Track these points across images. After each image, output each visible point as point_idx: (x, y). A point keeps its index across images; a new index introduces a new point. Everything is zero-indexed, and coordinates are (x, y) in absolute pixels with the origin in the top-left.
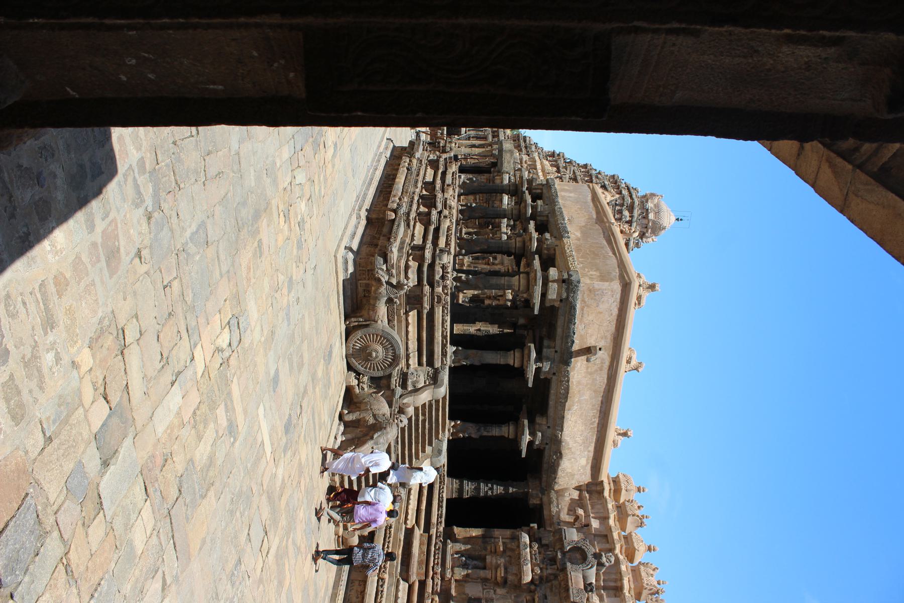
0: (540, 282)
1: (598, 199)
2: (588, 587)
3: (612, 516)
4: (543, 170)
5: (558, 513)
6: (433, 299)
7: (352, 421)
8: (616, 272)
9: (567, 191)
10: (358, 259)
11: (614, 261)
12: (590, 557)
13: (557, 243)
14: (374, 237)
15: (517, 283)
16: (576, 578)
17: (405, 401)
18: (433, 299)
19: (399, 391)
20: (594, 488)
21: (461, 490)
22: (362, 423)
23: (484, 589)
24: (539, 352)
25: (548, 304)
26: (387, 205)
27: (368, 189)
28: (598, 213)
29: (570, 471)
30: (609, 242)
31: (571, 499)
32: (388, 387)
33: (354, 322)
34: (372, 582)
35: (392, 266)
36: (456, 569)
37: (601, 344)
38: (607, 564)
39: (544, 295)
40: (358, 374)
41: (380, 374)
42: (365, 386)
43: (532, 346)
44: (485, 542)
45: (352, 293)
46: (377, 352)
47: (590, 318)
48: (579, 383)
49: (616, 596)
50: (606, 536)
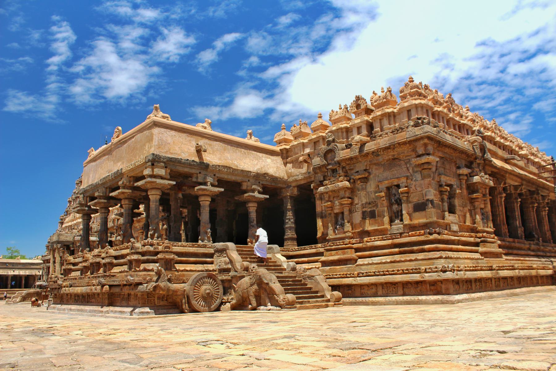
0: (154, 180)
1: (94, 158)
2: (349, 146)
3: (302, 141)
4: (73, 221)
5: (302, 174)
6: (167, 252)
7: (257, 301)
8: (146, 133)
9: (88, 180)
10: (140, 305)
11: (139, 136)
12: (330, 147)
13: (125, 176)
14: (123, 299)
15: (155, 196)
16: (343, 154)
17: (239, 268)
18: (167, 252)
19: (232, 273)
20: (285, 155)
21: (292, 239)
22: (257, 294)
23: (356, 211)
24: (201, 184)
25: (169, 177)
26: (98, 294)
27: (86, 311)
28: (104, 155)
29: (275, 169)
30: (125, 142)
31: (293, 168)
32: (230, 281)
33: (186, 307)
34: (361, 280)
35: (145, 279)
36: (346, 230)
37: (194, 143)
38: (333, 137)
39: (162, 178)
40: (222, 303)
41: (221, 287)
42: (230, 297)
43: (196, 188)
44: (326, 216)
45: (164, 309)
46: (206, 290)
47: (177, 149)
48: (220, 159)
49: (352, 131)
50: (315, 143)
